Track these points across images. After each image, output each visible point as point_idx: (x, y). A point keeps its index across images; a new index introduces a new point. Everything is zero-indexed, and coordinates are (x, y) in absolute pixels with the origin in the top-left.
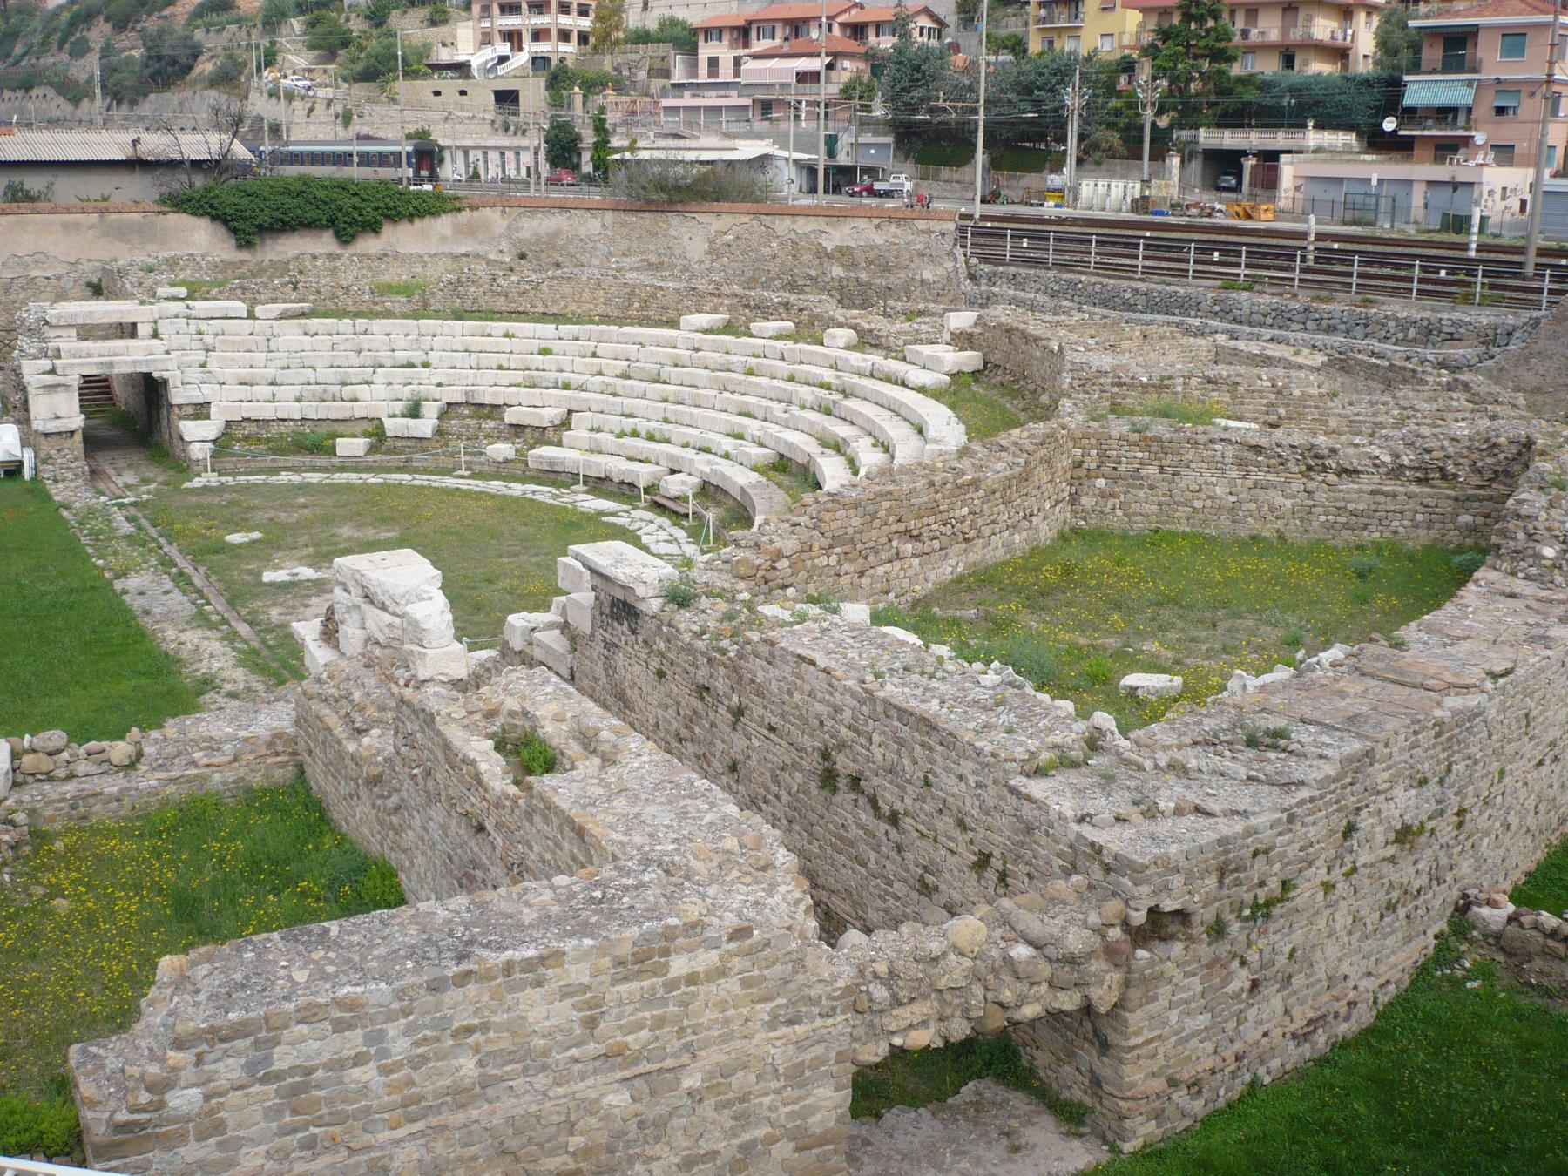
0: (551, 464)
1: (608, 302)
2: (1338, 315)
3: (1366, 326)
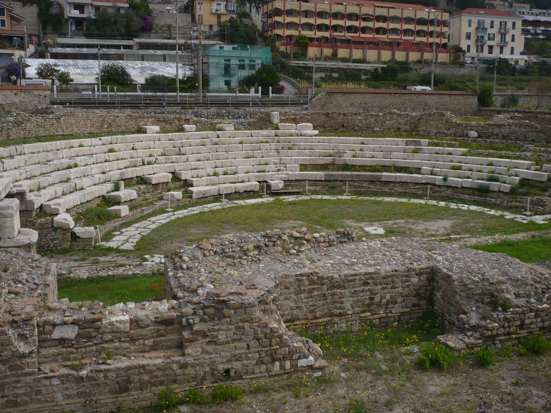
3: (251, 115)
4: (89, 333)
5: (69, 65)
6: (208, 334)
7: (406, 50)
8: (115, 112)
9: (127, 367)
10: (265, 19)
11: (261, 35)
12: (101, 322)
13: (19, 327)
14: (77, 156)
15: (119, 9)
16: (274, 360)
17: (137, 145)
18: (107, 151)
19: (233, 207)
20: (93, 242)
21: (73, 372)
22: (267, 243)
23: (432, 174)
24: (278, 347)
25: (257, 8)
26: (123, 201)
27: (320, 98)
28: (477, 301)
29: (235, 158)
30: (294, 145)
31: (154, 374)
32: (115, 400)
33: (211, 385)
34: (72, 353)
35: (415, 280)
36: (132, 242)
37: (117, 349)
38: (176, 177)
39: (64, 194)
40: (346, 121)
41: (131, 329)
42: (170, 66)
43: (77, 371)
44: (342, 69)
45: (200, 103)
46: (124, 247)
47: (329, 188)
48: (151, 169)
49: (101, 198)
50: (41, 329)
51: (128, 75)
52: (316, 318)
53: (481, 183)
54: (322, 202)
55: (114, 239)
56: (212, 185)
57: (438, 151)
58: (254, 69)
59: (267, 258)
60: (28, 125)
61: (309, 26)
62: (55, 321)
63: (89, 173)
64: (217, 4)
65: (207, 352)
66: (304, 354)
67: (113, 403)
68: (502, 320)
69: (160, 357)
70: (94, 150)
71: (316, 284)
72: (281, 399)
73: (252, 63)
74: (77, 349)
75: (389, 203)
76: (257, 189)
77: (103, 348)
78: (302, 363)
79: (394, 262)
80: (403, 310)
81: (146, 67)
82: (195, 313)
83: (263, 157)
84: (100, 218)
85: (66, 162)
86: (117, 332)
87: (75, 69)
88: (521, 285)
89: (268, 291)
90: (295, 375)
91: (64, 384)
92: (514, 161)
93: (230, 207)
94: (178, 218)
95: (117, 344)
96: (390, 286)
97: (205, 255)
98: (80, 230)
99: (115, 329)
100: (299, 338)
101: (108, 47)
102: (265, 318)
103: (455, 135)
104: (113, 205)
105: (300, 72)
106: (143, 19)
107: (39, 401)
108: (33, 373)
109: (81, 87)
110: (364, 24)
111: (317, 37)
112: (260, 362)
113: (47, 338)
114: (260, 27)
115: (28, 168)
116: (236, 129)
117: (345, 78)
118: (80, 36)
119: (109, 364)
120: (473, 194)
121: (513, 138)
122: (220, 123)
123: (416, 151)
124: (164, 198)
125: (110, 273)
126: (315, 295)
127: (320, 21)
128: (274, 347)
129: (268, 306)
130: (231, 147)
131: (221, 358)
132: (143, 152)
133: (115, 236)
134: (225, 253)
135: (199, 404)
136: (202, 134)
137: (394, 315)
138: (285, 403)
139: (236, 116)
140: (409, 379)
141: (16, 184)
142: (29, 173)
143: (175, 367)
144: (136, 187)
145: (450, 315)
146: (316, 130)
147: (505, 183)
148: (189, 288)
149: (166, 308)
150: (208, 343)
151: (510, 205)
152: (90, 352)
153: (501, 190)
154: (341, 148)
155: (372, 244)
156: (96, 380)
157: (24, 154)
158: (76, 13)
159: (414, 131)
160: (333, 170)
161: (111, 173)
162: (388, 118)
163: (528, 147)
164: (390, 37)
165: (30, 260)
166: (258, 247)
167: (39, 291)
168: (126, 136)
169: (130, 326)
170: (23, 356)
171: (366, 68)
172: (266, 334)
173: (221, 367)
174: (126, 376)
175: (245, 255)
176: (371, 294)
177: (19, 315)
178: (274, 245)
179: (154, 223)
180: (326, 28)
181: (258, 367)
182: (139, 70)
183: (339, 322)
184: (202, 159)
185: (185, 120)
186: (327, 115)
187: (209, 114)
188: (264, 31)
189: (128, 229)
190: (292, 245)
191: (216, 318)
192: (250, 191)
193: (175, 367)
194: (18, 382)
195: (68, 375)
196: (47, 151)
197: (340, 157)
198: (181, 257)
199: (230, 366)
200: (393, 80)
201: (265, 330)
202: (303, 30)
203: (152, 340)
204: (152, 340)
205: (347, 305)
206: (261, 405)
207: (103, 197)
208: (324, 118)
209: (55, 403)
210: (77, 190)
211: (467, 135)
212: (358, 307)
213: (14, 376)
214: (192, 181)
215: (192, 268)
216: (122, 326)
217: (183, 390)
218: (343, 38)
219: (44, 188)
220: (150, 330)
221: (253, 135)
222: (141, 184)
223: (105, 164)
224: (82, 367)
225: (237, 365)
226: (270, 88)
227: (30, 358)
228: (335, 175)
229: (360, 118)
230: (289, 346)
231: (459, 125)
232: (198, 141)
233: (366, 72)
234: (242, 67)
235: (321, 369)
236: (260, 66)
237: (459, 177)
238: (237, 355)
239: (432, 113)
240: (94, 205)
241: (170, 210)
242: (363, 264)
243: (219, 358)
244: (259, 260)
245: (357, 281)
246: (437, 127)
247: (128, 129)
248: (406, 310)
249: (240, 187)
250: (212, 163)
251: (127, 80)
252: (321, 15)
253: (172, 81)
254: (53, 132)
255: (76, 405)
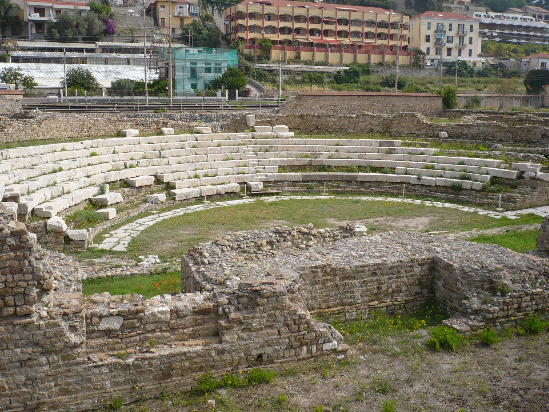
0: (187, 196)
1: (73, 129)
2: (213, 116)
3: (223, 118)
4: (133, 324)
5: (32, 69)
6: (244, 321)
7: (367, 52)
8: (94, 116)
9: (169, 355)
10: (228, 22)
11: (224, 38)
12: (144, 313)
13: (69, 319)
14: (61, 160)
15: (80, 12)
16: (301, 345)
17: (118, 149)
18: (89, 155)
19: (216, 208)
20: (86, 244)
21: (120, 361)
22: (279, 238)
23: (406, 174)
24: (306, 332)
25: (220, 11)
26: (109, 204)
27: (291, 101)
28: (477, 287)
29: (215, 161)
30: (271, 147)
31: (195, 360)
32: (159, 385)
33: (246, 369)
34: (118, 343)
35: (418, 270)
36: (124, 244)
37: (159, 338)
38: (158, 180)
39: (53, 198)
40: (320, 123)
41: (171, 319)
42: (134, 70)
43: (123, 360)
44: (306, 72)
45: (170, 107)
46: (117, 248)
47: (307, 188)
48: (134, 172)
49: (88, 202)
50: (89, 320)
51: (93, 79)
52: (330, 307)
53: (454, 181)
54: (302, 202)
55: (105, 241)
56: (194, 187)
57: (410, 151)
58: (220, 72)
59: (280, 253)
60: (10, 130)
61: (273, 30)
62: (102, 313)
63: (74, 177)
64: (180, 7)
65: (243, 339)
66: (329, 338)
67: (157, 389)
68: (502, 303)
69: (199, 345)
70: (77, 154)
71: (329, 275)
72: (311, 380)
73: (219, 66)
74: (122, 339)
75: (367, 202)
76: (238, 190)
77: (146, 337)
78: (327, 347)
79: (398, 254)
80: (407, 298)
81: (110, 71)
82: (230, 303)
83: (241, 159)
84: (89, 221)
85: (51, 166)
86: (158, 322)
87: (38, 73)
88: (516, 272)
89: (294, 281)
90: (321, 359)
91: (112, 372)
92: (484, 160)
93: (213, 209)
94: (164, 220)
95: (159, 333)
96: (395, 276)
97: (223, 251)
98: (72, 233)
99: (157, 319)
100: (323, 324)
101: (70, 50)
102: (294, 306)
103: (426, 135)
104: (100, 208)
105: (265, 75)
106: (105, 22)
107: (89, 389)
108: (84, 363)
109: (45, 92)
110: (326, 27)
111: (280, 40)
112: (290, 347)
113: (94, 330)
114: (223, 31)
115: (16, 172)
116: (213, 132)
117: (308, 81)
118: (41, 39)
119: (153, 353)
120: (447, 192)
121: (482, 138)
122: (198, 126)
123: (390, 151)
124: (148, 200)
125: (109, 273)
126: (328, 286)
127: (282, 24)
128: (302, 333)
129: (295, 295)
130: (210, 149)
131: (255, 344)
132: (125, 156)
133: (105, 238)
134: (241, 248)
135: (234, 387)
136: (180, 137)
137: (399, 303)
138: (314, 384)
139: (209, 119)
140: (423, 359)
141: (7, 188)
142: (17, 178)
143: (213, 353)
144: (120, 190)
145: (452, 302)
146: (293, 131)
147: (476, 181)
148: (216, 281)
149: (202, 299)
150: (243, 330)
151: (482, 202)
152: (133, 342)
153: (473, 188)
154: (317, 150)
155: (373, 238)
156: (142, 367)
157: (9, 158)
158: (36, 16)
159: (386, 132)
160: (310, 171)
161: (95, 176)
162: (361, 120)
163: (496, 147)
164: (352, 39)
165: (58, 258)
166: (270, 243)
167: (73, 287)
168: (106, 139)
169: (171, 317)
170: (76, 346)
171: (330, 71)
172: (295, 320)
173: (255, 353)
174: (169, 363)
175: (259, 250)
176: (379, 284)
177: (69, 307)
178: (284, 241)
179: (141, 225)
180: (289, 31)
181: (288, 351)
182: (103, 74)
183: (350, 310)
184: (182, 162)
185: (163, 123)
186: (302, 117)
187: (182, 117)
188: (227, 34)
189: (117, 231)
190: (300, 240)
191: (249, 307)
192: (231, 193)
193: (213, 353)
194: (69, 371)
195: (115, 364)
196: (31, 156)
197: (317, 158)
198: (201, 254)
199: (262, 351)
200: (356, 82)
201: (294, 317)
202: (266, 33)
203: (191, 329)
204: (191, 329)
205: (358, 295)
206: (293, 387)
207: (90, 200)
208: (298, 120)
209: (104, 391)
210: (64, 194)
211: (438, 136)
212: (367, 296)
213: (66, 365)
214: (175, 183)
215: (213, 262)
216: (163, 317)
217: (220, 374)
218: (306, 41)
219: (33, 192)
220: (189, 319)
221: (231, 137)
222: (124, 187)
223: (90, 168)
224: (128, 355)
225: (269, 350)
226: (237, 91)
227: (80, 348)
228: (313, 175)
229: (334, 120)
230: (315, 331)
231: (430, 126)
232: (177, 144)
233: (329, 74)
234: (208, 70)
235: (344, 352)
236: (226, 69)
237: (433, 176)
238: (269, 341)
239: (404, 115)
240: (81, 208)
241: (155, 212)
242: (370, 256)
243: (253, 344)
244: (273, 254)
245: (366, 272)
246: (409, 128)
247: (107, 133)
248: (411, 298)
249: (222, 188)
250: (192, 166)
251: (93, 83)
252: (283, 18)
253: (140, 85)
254: (34, 136)
255: (124, 391)
